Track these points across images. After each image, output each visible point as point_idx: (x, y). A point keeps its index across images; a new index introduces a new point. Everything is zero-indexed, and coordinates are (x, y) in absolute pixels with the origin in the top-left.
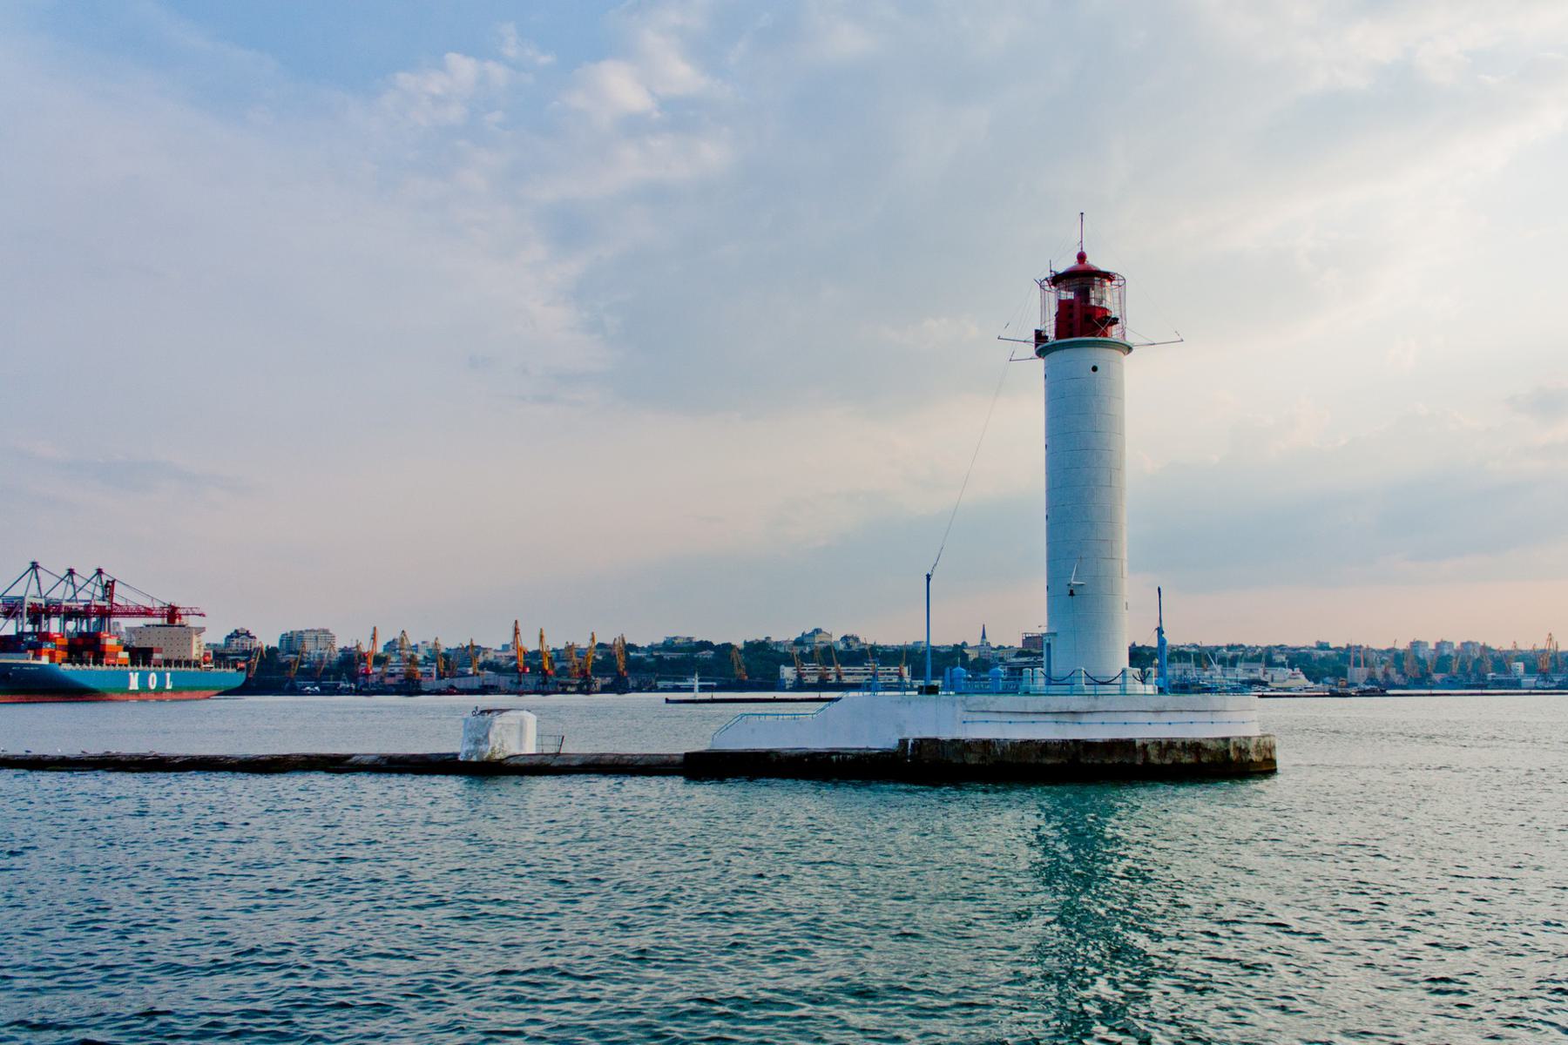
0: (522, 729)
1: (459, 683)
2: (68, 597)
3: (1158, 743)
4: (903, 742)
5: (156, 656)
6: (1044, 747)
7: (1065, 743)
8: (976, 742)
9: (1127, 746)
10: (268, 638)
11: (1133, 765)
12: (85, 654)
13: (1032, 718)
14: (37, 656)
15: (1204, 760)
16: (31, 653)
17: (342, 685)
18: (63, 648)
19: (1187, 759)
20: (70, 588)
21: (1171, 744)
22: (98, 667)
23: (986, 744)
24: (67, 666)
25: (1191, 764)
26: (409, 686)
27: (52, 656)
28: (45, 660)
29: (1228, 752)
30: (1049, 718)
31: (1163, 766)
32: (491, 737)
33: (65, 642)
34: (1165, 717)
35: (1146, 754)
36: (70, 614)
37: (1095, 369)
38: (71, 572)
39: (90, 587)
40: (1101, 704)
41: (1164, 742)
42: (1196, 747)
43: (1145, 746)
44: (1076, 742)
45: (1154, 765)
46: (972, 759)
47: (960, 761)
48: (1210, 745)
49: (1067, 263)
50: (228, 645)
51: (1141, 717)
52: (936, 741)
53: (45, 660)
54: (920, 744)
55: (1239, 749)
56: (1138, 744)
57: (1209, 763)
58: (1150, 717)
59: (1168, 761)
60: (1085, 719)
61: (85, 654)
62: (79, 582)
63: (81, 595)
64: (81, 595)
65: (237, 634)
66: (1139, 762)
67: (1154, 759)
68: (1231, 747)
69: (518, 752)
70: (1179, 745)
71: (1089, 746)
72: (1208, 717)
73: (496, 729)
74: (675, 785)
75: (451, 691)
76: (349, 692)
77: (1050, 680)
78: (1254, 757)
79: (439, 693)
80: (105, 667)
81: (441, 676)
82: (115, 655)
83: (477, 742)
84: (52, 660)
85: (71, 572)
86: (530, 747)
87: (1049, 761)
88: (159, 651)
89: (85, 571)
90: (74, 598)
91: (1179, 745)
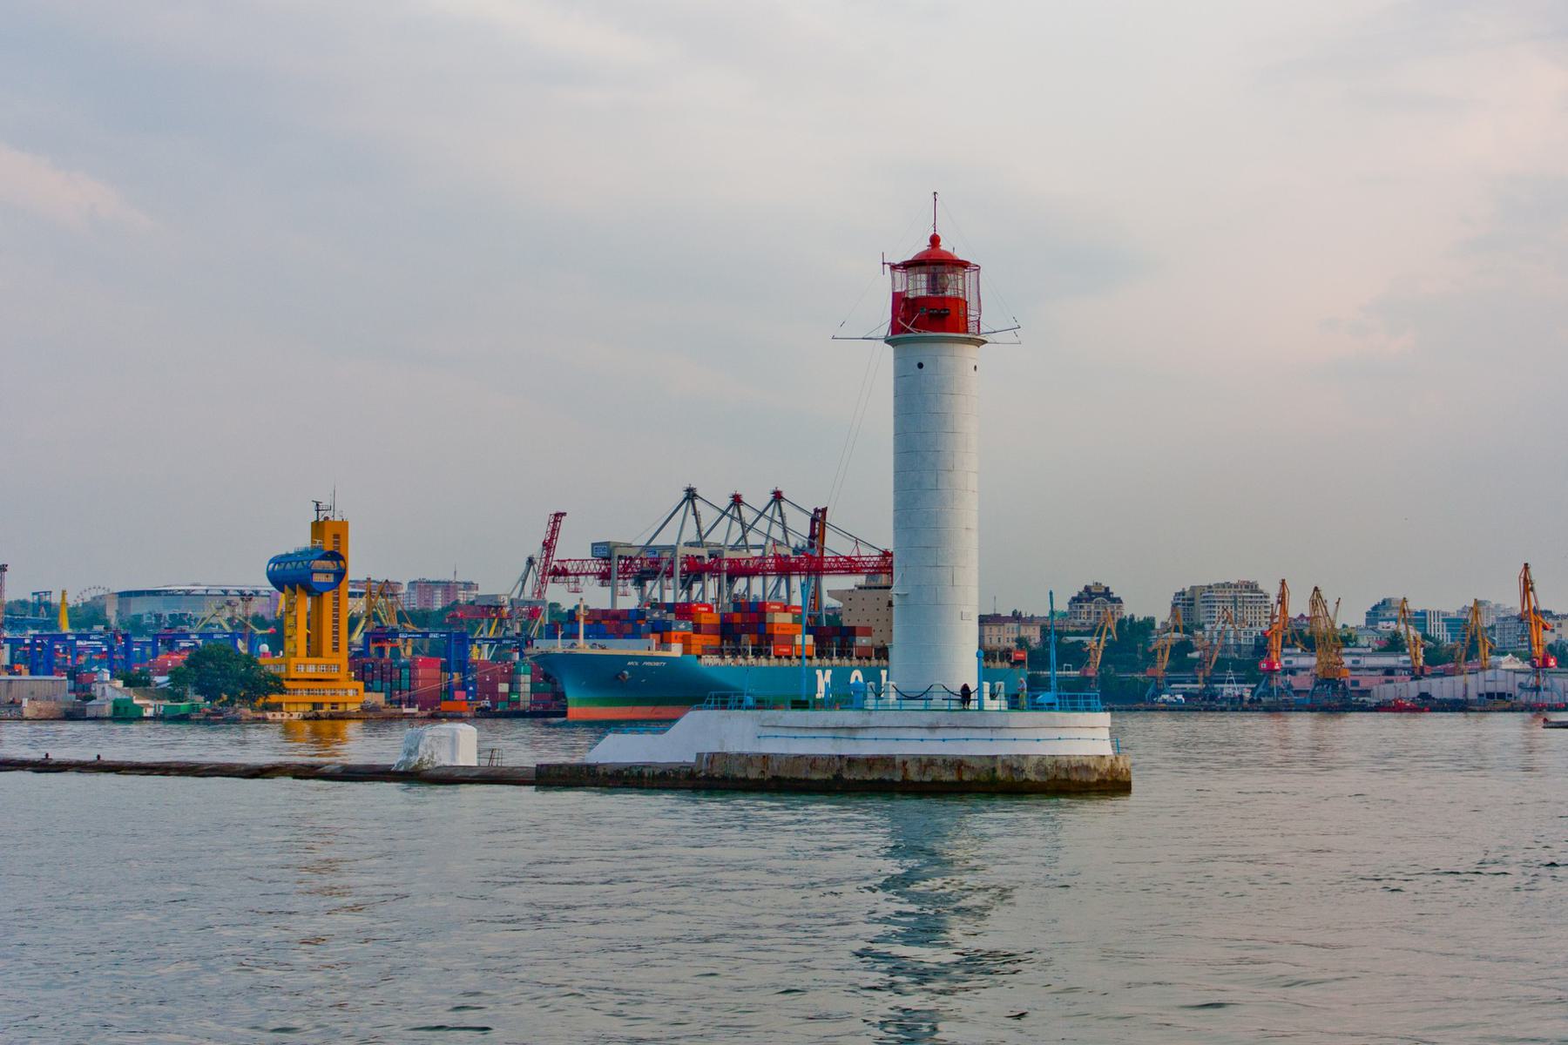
0: (454, 741)
1: (1442, 688)
2: (732, 542)
3: (917, 759)
4: (699, 755)
5: (862, 641)
6: (813, 762)
7: (831, 758)
8: (757, 755)
9: (887, 761)
10: (1147, 601)
11: (892, 782)
12: (745, 638)
13: (814, 733)
14: (664, 643)
15: (966, 777)
16: (654, 640)
17: (1229, 690)
18: (712, 630)
19: (948, 776)
20: (737, 526)
21: (930, 762)
22: (763, 661)
23: (766, 758)
24: (710, 660)
25: (952, 783)
26: (1335, 698)
27: (686, 642)
28: (676, 650)
29: (994, 770)
30: (828, 733)
31: (921, 782)
32: (421, 748)
33: (714, 619)
34: (939, 734)
35: (906, 770)
36: (738, 570)
37: (920, 366)
38: (737, 500)
39: (763, 524)
40: (874, 719)
41: (925, 760)
42: (958, 764)
43: (904, 763)
44: (840, 757)
45: (913, 782)
46: (753, 774)
47: (741, 775)
48: (975, 764)
49: (917, 246)
50: (1072, 614)
51: (915, 734)
52: (726, 755)
53: (676, 650)
54: (713, 757)
55: (1011, 768)
56: (898, 761)
57: (969, 783)
58: (925, 734)
59: (927, 779)
60: (860, 734)
61: (745, 638)
62: (749, 516)
63: (753, 538)
64: (753, 538)
65: (1088, 595)
66: (898, 779)
67: (914, 775)
68: (999, 765)
69: (448, 763)
70: (940, 762)
71: (852, 761)
72: (987, 734)
73: (427, 740)
74: (528, 792)
75: (1426, 704)
76: (1237, 705)
77: (904, 696)
78: (1032, 777)
79: (1395, 707)
80: (774, 662)
81: (1416, 674)
82: (790, 640)
83: (410, 753)
84: (686, 652)
85: (737, 500)
86: (472, 761)
87: (816, 776)
88: (867, 632)
89: (757, 498)
90: (743, 544)
91: (940, 762)
